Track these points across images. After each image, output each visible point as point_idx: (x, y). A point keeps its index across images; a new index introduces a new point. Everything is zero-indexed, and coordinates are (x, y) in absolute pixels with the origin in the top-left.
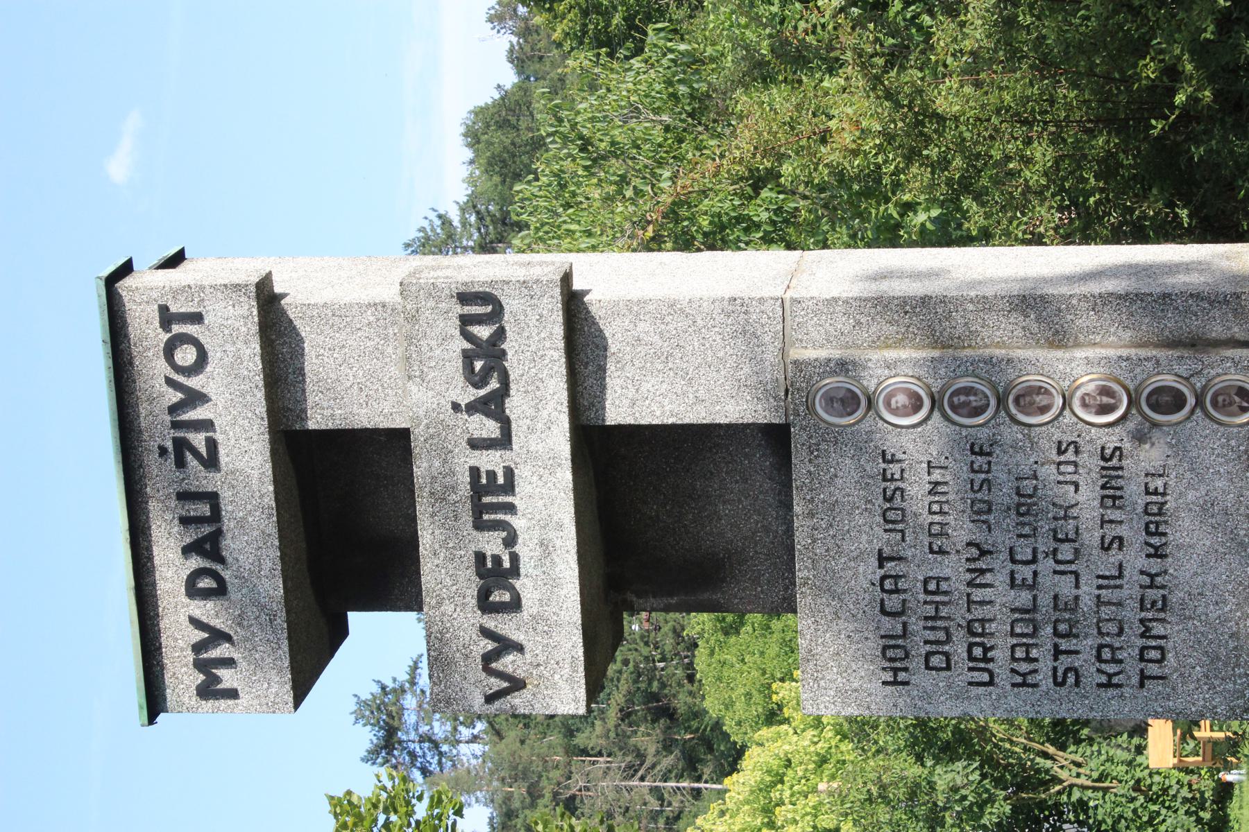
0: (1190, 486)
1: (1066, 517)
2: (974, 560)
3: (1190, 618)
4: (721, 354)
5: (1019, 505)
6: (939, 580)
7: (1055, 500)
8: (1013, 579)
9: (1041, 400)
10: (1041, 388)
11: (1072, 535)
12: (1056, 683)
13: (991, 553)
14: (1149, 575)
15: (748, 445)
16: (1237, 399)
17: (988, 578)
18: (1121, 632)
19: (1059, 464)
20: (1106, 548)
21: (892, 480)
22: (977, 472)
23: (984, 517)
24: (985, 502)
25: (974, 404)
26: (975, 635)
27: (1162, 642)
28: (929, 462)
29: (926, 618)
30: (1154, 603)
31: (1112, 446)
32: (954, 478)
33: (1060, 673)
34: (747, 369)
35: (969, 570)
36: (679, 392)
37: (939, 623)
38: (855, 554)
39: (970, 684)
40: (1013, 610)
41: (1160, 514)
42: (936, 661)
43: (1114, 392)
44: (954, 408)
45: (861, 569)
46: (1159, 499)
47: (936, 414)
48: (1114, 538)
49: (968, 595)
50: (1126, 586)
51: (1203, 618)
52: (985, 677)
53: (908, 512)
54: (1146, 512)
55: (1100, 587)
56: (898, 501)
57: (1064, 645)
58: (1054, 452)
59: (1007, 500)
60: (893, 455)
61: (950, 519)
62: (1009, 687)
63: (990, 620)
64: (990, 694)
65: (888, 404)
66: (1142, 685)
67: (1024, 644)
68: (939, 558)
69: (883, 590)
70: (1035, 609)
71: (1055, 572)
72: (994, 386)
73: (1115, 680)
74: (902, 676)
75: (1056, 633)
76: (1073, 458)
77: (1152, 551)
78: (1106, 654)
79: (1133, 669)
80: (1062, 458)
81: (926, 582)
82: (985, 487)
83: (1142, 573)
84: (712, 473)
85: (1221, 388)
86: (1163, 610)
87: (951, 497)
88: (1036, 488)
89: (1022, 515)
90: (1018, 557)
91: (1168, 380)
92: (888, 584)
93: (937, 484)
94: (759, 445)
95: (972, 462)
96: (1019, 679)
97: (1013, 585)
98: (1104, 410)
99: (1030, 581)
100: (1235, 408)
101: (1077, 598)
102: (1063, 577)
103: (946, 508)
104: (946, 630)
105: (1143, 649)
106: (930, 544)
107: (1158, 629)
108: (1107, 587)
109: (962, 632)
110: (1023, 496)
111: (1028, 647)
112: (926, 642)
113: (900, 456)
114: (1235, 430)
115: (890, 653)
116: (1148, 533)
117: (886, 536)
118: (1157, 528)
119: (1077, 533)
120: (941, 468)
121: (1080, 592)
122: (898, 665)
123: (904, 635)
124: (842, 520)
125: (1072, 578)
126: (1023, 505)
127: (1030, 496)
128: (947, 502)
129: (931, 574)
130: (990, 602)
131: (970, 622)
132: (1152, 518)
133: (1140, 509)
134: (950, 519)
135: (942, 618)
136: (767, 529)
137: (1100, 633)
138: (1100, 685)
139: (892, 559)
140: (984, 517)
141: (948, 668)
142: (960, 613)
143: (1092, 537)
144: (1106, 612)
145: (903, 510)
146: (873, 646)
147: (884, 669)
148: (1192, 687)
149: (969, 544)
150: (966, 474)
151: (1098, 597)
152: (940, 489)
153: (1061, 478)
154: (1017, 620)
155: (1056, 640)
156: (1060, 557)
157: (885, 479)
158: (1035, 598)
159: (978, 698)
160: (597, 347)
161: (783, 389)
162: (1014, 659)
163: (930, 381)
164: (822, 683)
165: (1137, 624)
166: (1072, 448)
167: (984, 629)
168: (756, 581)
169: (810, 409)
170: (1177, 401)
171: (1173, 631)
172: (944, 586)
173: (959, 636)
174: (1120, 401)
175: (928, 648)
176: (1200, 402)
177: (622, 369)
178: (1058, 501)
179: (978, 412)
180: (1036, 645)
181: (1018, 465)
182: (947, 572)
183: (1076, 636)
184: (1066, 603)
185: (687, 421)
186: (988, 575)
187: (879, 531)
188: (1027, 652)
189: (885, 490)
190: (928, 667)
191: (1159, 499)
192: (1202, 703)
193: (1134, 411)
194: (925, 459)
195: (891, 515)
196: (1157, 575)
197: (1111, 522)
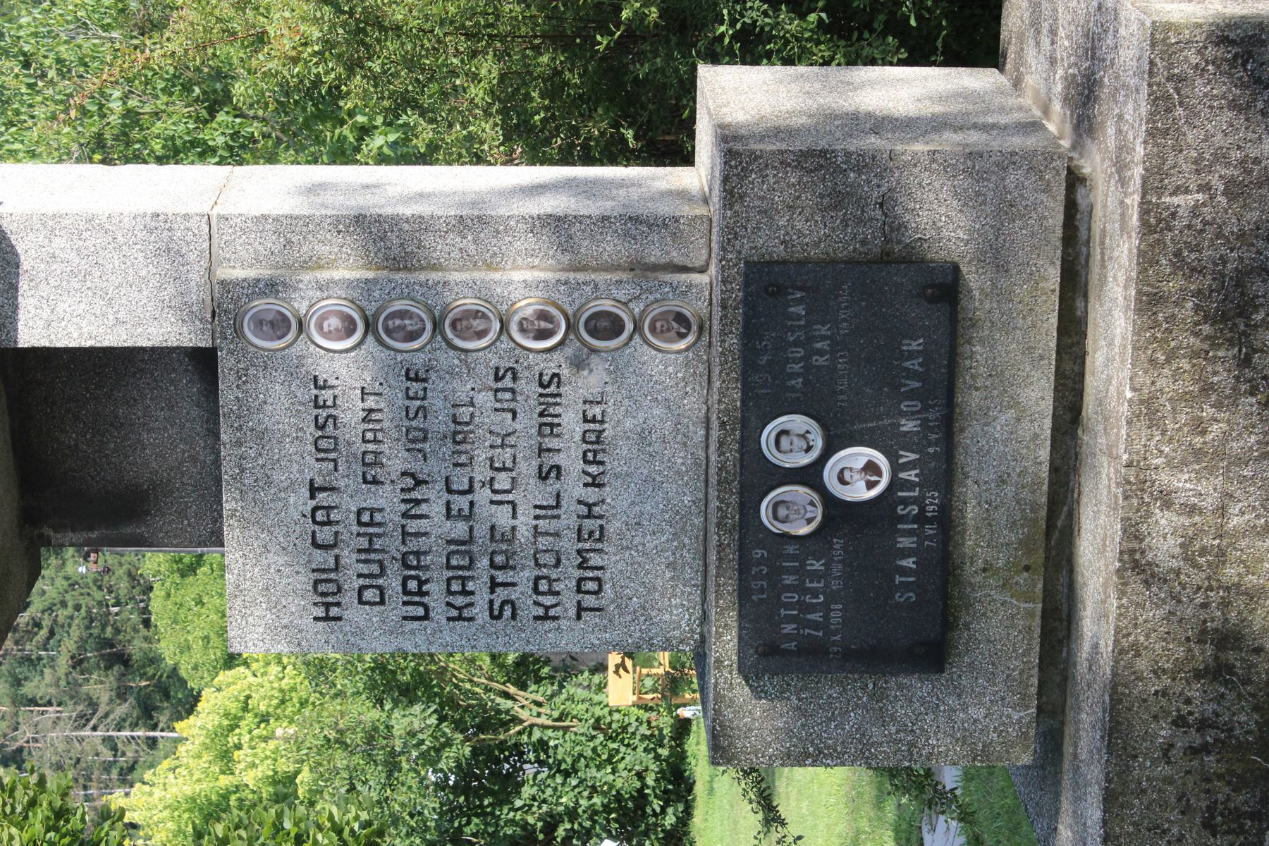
0: (628, 413)
1: (503, 446)
2: (409, 490)
3: (628, 548)
4: (143, 273)
5: (455, 433)
6: (372, 511)
7: (492, 428)
9: (478, 324)
10: (478, 311)
11: (509, 464)
12: (492, 617)
13: (426, 482)
14: (587, 504)
15: (174, 370)
16: (675, 324)
17: (423, 509)
18: (558, 563)
19: (497, 390)
20: (543, 477)
21: (324, 406)
22: (412, 399)
23: (419, 446)
24: (420, 430)
25: (410, 328)
27: (599, 573)
28: (363, 388)
29: (359, 551)
30: (591, 533)
31: (550, 372)
32: (389, 405)
33: (496, 606)
34: (171, 290)
35: (404, 501)
36: (98, 313)
37: (373, 556)
38: (285, 484)
39: (405, 618)
40: (449, 542)
41: (597, 442)
42: (369, 595)
43: (552, 317)
44: (388, 332)
45: (292, 500)
46: (597, 426)
47: (370, 339)
48: (552, 467)
49: (403, 527)
50: (563, 517)
51: (640, 548)
52: (420, 611)
53: (341, 440)
54: (584, 441)
55: (537, 517)
56: (330, 428)
57: (501, 577)
58: (492, 378)
59: (443, 428)
60: (325, 381)
61: (384, 448)
62: (444, 621)
63: (426, 553)
64: (425, 629)
65: (320, 328)
66: (579, 617)
67: (460, 577)
68: (373, 488)
69: (314, 522)
71: (492, 502)
72: (430, 310)
73: (552, 612)
74: (334, 611)
75: (493, 565)
76: (510, 385)
77: (590, 480)
78: (543, 586)
79: (569, 601)
80: (500, 385)
81: (359, 513)
82: (420, 415)
83: (580, 502)
84: (135, 400)
85: (661, 314)
86: (600, 540)
87: (386, 425)
88: (472, 415)
89: (459, 443)
90: (455, 487)
91: (607, 305)
92: (320, 516)
93: (371, 411)
94: (187, 370)
95: (408, 389)
96: (455, 613)
97: (449, 515)
98: (542, 335)
99: (466, 512)
100: (673, 334)
101: (514, 528)
102: (500, 507)
103: (380, 436)
104: (380, 563)
105: (580, 581)
106: (364, 474)
107: (595, 560)
108: (544, 517)
109: (397, 565)
110: (460, 423)
111: (464, 580)
112: (359, 576)
113: (332, 382)
114: (673, 356)
117: (318, 465)
118: (595, 456)
119: (514, 461)
120: (376, 394)
121: (516, 522)
122: (330, 599)
123: (336, 569)
124: (272, 449)
125: (509, 508)
126: (460, 433)
127: (467, 424)
128: (381, 430)
129: (365, 505)
130: (425, 534)
131: (404, 555)
132: (590, 447)
133: (578, 437)
134: (384, 448)
135: (375, 551)
136: (194, 460)
137: (537, 564)
138: (537, 618)
139: (324, 489)
140: (419, 446)
141: (382, 602)
142: (394, 546)
144: (543, 542)
145: (335, 438)
146: (304, 581)
147: (315, 604)
148: (629, 618)
149: (403, 474)
150: (401, 401)
151: (536, 527)
152: (374, 416)
153: (498, 405)
154: (453, 552)
155: (493, 572)
156: (497, 486)
157: (317, 406)
158: (471, 529)
159: (413, 632)
160: (9, 263)
161: (209, 311)
162: (450, 592)
163: (364, 304)
164: (250, 619)
165: (575, 554)
166: (509, 374)
167: (419, 561)
168: (182, 514)
169: (238, 332)
172: (378, 517)
173: (394, 569)
174: (559, 326)
175: (361, 581)
176: (637, 328)
177: (36, 287)
178: (496, 429)
179: (412, 336)
180: (472, 578)
181: (454, 391)
182: (381, 503)
183: (513, 568)
184: (503, 534)
185: (106, 344)
186: (424, 506)
188: (464, 585)
189: (316, 417)
190: (361, 602)
191: (597, 426)
192: (638, 634)
193: (572, 337)
194: (359, 385)
195: (323, 444)
196: (595, 504)
197: (549, 450)
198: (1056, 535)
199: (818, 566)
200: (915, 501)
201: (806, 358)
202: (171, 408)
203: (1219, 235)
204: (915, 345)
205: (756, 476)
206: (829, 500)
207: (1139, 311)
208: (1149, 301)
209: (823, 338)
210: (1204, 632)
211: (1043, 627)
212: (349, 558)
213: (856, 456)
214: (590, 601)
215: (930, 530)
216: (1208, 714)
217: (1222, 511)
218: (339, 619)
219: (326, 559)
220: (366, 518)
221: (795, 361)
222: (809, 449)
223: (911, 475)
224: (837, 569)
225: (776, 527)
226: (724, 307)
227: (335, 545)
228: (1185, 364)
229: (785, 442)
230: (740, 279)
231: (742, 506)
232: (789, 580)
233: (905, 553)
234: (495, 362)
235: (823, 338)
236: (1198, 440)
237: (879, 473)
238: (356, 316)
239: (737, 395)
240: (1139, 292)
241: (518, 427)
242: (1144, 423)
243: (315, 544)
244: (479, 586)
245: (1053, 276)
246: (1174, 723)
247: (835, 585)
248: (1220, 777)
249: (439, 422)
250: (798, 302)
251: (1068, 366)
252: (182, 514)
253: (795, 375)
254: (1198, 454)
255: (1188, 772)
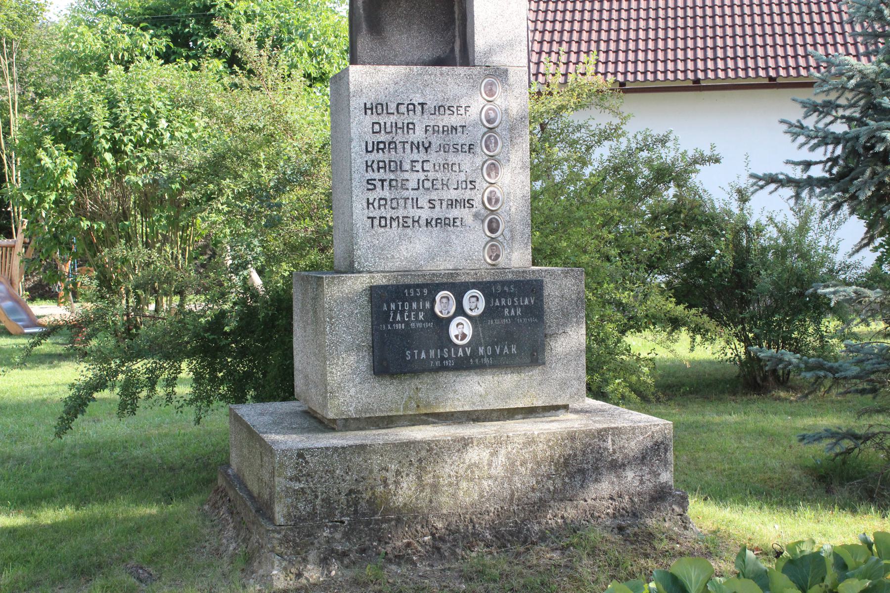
1: (443, 184)
6: (414, 129)
8: (415, 161)
12: (368, 180)
17: (415, 151)
26: (389, 145)
27: (389, 226)
30: (406, 222)
37: (394, 129)
42: (377, 127)
44: (490, 136)
47: (486, 130)
52: (370, 149)
55: (413, 199)
56: (448, 112)
57: (386, 184)
59: (450, 159)
65: (490, 109)
66: (369, 218)
70: (402, 171)
72: (498, 154)
73: (371, 206)
74: (369, 112)
75: (391, 180)
78: (382, 202)
79: (376, 213)
81: (412, 123)
91: (501, 227)
92: (411, 107)
93: (456, 130)
96: (369, 164)
97: (412, 161)
98: (490, 200)
107: (395, 224)
109: (390, 140)
111: (385, 168)
115: (379, 107)
116: (437, 219)
133: (447, 216)
137: (392, 200)
141: (374, 133)
142: (399, 138)
143: (434, 195)
144: (402, 202)
150: (461, 142)
152: (454, 131)
159: (360, 146)
162: (379, 162)
168: (372, 49)
169: (487, 76)
170: (492, 230)
171: (394, 231)
172: (411, 131)
175: (383, 124)
179: (487, 147)
182: (417, 133)
187: (435, 104)
190: (373, 123)
195: (442, 109)
198: (425, 418)
199: (421, 317)
200: (450, 356)
201: (507, 306)
202: (417, 47)
203: (597, 460)
204: (514, 350)
205: (459, 290)
206: (450, 320)
207: (568, 433)
208: (572, 436)
209: (516, 313)
210: (438, 477)
211: (384, 417)
212: (393, 119)
213: (468, 329)
214: (376, 222)
215: (438, 363)
216: (402, 484)
217: (490, 478)
218: (366, 113)
219: (392, 108)
220: (411, 126)
221: (506, 302)
222: (471, 310)
223: (461, 353)
224: (419, 325)
225: (438, 298)
226: (523, 272)
227: (398, 112)
228: (548, 453)
229: (474, 299)
230: (534, 278)
231: (446, 283)
232: (414, 305)
233: (427, 353)
234: (478, 181)
235: (516, 313)
236: (518, 463)
237: (462, 340)
238: (496, 124)
239: (488, 279)
240: (576, 432)
241: (452, 191)
242: (525, 440)
243: (398, 104)
244: (382, 174)
245: (539, 403)
246: (398, 470)
247: (412, 325)
248: (373, 494)
249: (452, 158)
250: (530, 302)
251: (495, 415)
252: (372, 49)
253: (500, 301)
254: (513, 464)
255: (375, 480)
